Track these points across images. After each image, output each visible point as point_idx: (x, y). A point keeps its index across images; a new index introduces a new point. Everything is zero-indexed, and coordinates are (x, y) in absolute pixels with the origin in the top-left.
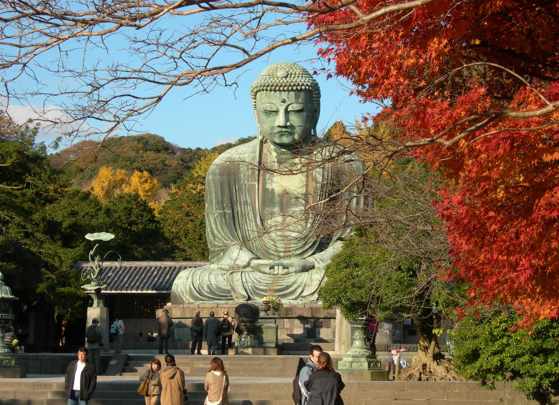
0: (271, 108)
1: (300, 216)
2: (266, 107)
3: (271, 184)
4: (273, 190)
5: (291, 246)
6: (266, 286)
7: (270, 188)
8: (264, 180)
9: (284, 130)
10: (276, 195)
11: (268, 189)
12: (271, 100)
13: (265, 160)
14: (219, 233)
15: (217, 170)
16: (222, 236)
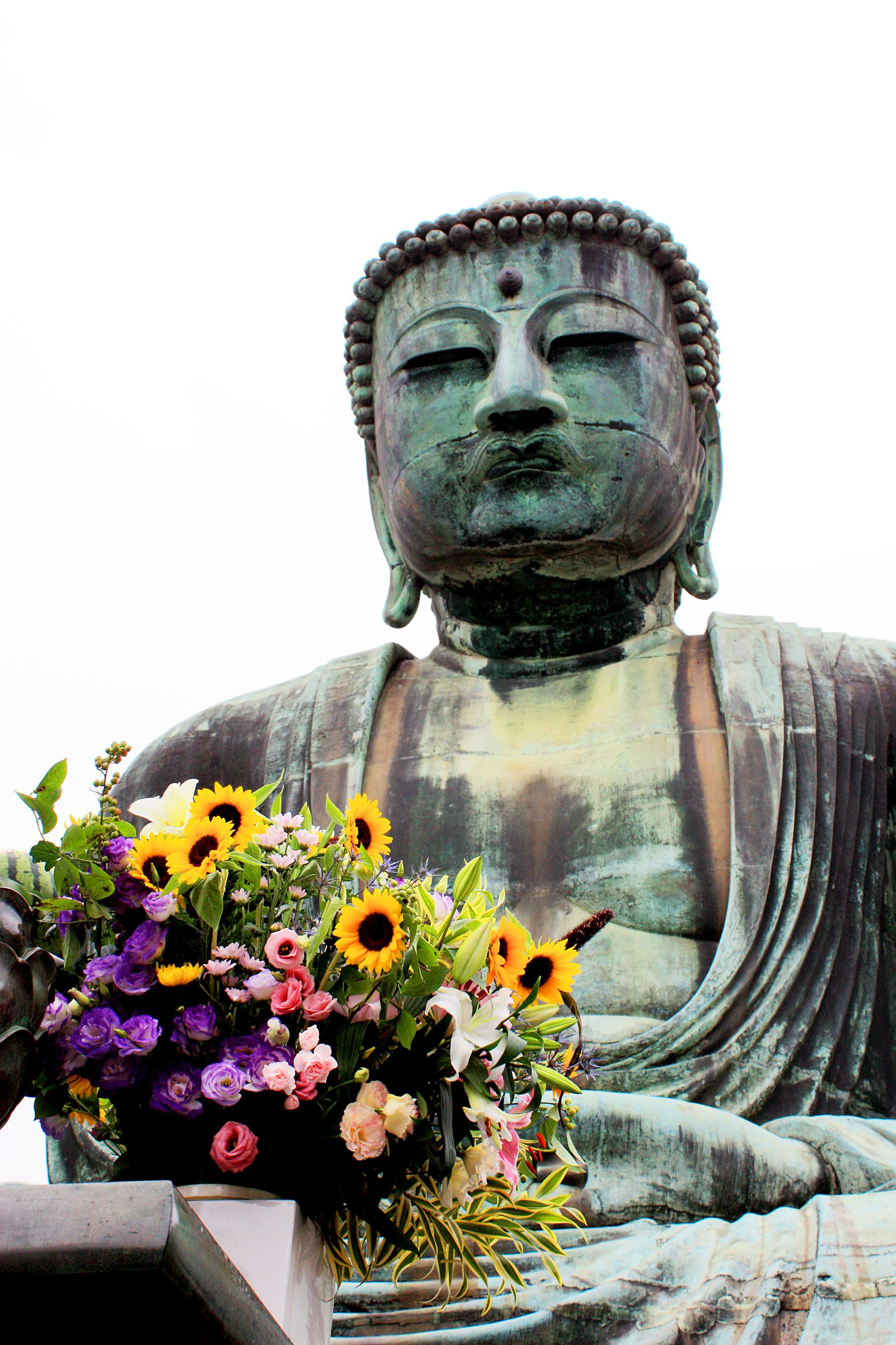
0: (446, 336)
2: (421, 342)
8: (407, 750)
9: (521, 442)
10: (481, 805)
11: (427, 781)
12: (444, 300)
13: (421, 687)
15: (142, 771)
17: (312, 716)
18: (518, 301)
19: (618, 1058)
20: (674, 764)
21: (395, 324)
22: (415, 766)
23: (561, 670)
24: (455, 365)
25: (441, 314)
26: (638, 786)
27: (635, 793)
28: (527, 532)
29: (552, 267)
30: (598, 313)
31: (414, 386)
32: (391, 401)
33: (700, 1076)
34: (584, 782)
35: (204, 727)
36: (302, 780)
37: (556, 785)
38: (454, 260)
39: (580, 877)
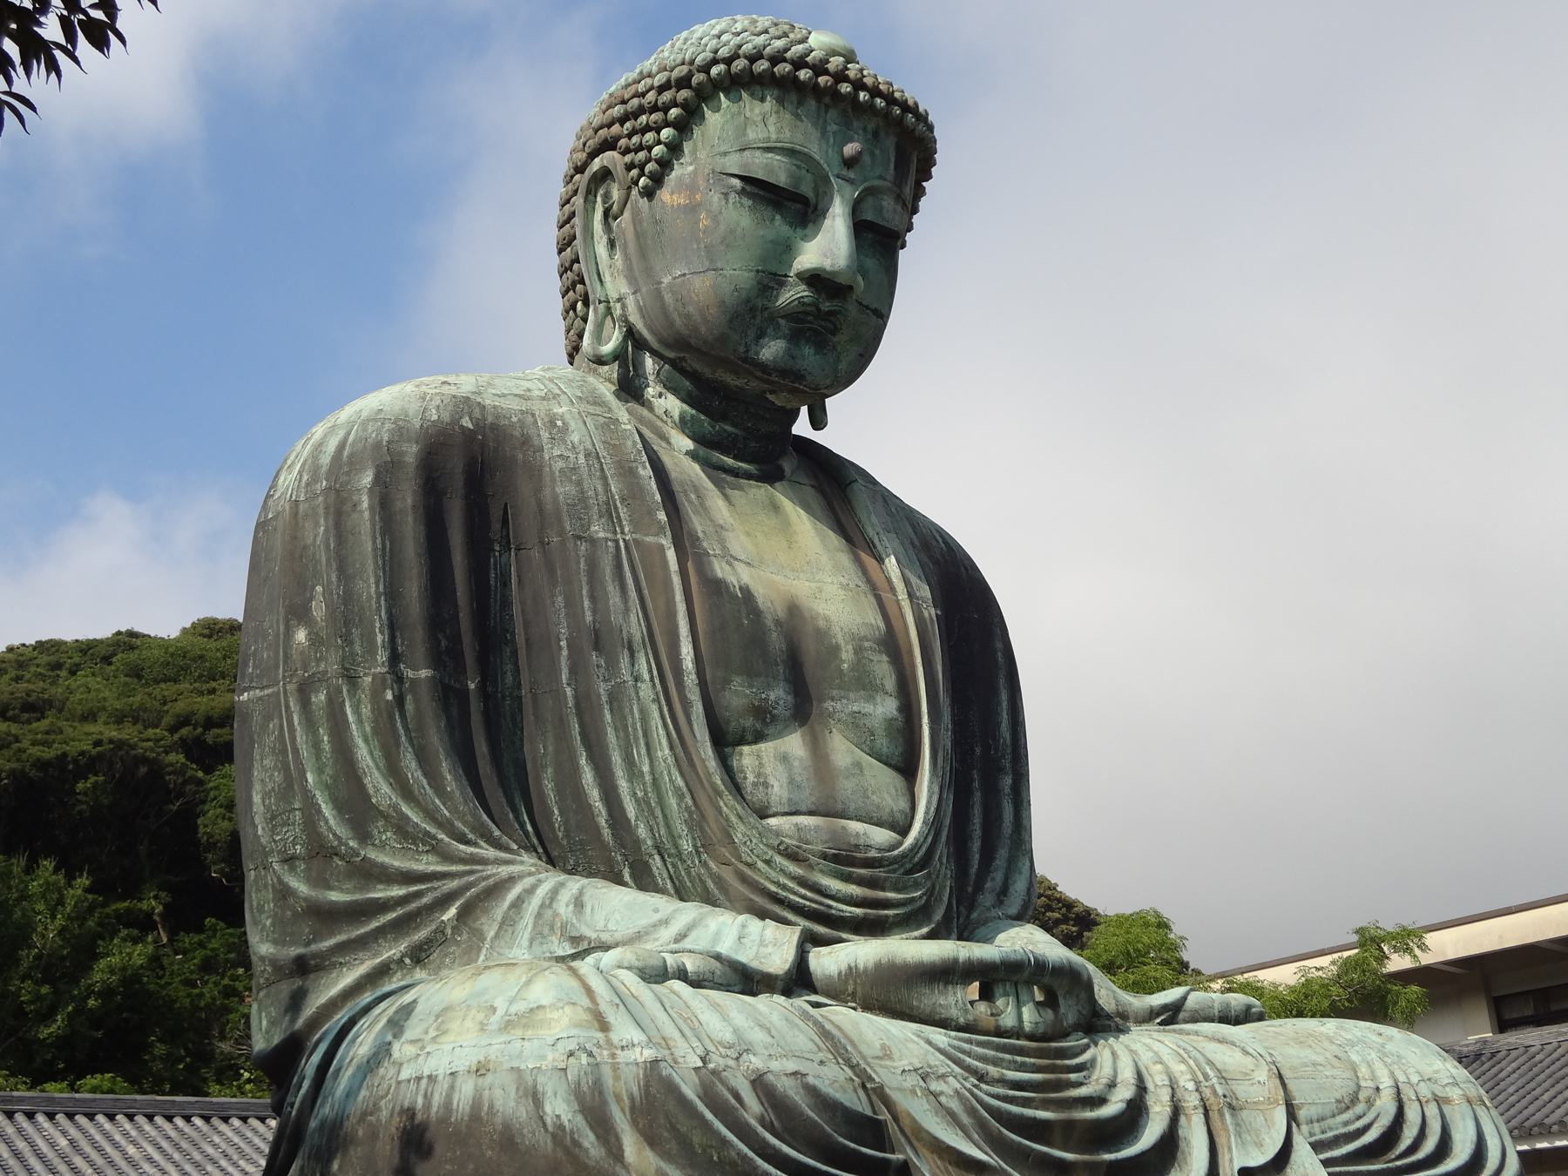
1: (883, 743)
2: (768, 168)
3: (728, 563)
4: (746, 591)
5: (891, 895)
6: (1026, 1103)
7: (731, 579)
10: (769, 622)
14: (407, 792)
16: (431, 815)
17: (602, 470)
18: (851, 175)
19: (891, 864)
20: (882, 625)
21: (742, 130)
22: (710, 563)
23: (749, 476)
24: (789, 204)
25: (791, 152)
26: (865, 638)
27: (866, 644)
28: (798, 376)
29: (877, 152)
30: (895, 211)
31: (747, 202)
32: (716, 198)
33: (929, 884)
34: (827, 619)
35: (466, 422)
36: (616, 542)
37: (807, 614)
38: (812, 103)
39: (839, 706)
